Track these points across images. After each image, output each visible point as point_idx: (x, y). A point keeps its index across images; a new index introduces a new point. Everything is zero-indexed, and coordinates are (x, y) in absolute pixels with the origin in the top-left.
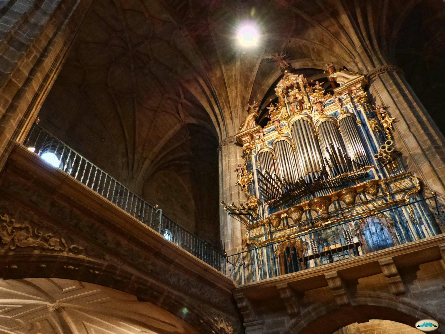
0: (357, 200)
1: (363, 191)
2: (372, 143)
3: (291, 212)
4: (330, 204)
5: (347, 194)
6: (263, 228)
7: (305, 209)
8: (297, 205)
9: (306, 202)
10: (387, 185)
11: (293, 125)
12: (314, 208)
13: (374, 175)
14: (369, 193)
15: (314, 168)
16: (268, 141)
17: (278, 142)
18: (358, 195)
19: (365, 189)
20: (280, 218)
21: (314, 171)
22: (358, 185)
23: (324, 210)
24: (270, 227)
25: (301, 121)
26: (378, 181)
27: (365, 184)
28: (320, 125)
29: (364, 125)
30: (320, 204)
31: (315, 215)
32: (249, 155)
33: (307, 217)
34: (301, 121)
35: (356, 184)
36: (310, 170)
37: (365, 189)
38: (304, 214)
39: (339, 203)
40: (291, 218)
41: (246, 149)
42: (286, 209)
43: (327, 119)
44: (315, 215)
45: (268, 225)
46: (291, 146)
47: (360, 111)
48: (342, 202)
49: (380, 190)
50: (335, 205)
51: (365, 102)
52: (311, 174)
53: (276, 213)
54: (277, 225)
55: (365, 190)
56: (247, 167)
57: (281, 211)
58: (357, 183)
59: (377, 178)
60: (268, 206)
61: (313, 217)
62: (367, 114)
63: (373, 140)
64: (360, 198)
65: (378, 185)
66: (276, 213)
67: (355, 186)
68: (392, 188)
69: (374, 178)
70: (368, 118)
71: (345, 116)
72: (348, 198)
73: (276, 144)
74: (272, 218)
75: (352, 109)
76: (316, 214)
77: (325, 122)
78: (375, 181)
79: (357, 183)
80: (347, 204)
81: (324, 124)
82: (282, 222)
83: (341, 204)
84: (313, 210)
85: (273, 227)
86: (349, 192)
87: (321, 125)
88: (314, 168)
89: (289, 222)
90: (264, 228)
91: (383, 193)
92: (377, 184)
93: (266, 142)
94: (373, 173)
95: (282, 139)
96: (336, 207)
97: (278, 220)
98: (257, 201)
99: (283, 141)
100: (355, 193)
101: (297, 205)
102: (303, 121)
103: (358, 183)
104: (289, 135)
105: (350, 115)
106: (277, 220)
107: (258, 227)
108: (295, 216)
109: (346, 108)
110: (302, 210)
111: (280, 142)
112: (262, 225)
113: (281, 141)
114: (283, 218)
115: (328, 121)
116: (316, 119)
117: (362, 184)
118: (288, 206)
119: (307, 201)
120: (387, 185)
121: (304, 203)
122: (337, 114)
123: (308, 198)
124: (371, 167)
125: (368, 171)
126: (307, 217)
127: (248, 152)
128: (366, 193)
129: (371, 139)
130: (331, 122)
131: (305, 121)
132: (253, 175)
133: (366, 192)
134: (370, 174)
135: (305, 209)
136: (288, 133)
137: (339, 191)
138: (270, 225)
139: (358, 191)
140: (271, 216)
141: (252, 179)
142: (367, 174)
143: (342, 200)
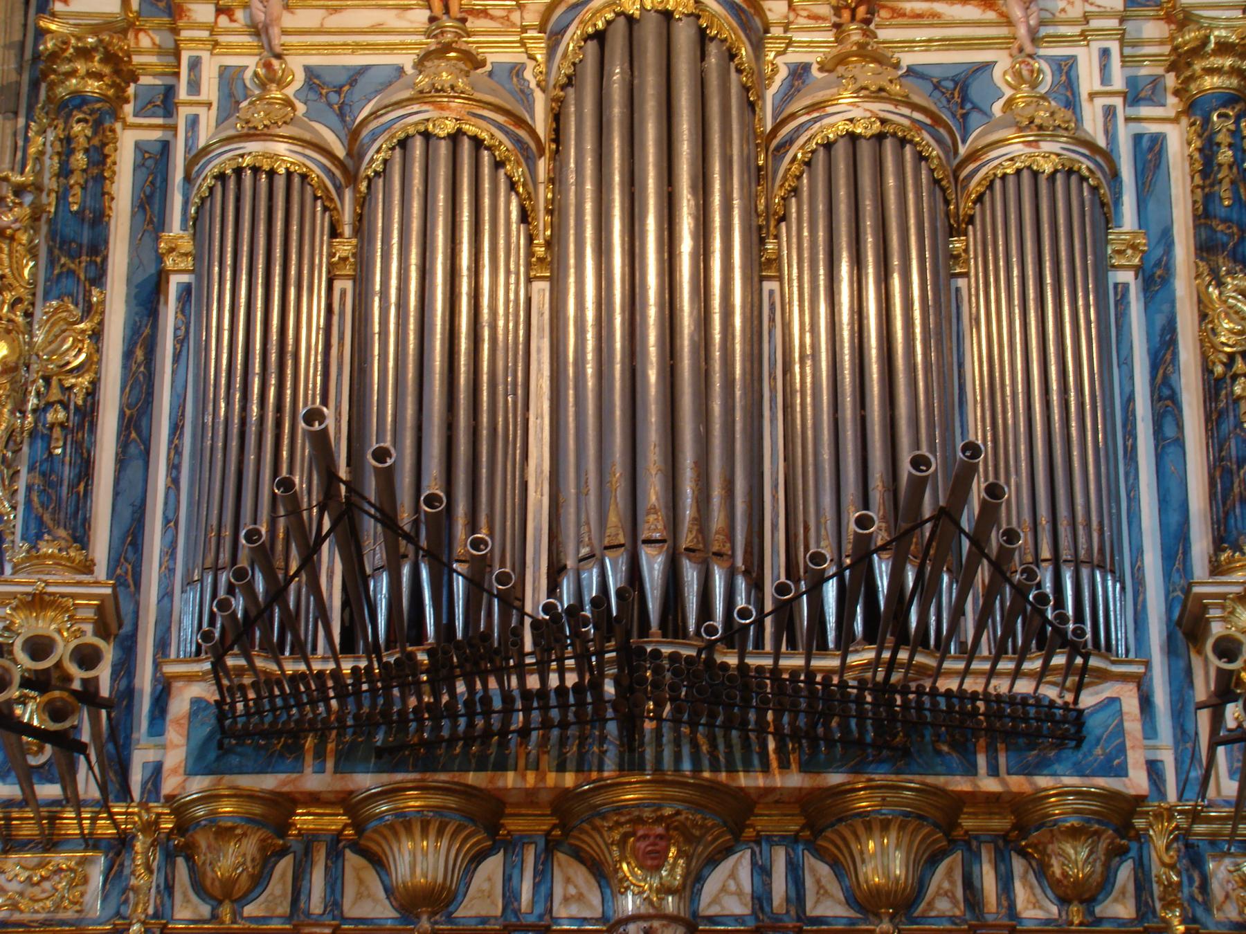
0: (940, 893)
1: (1005, 837)
2: (1170, 467)
3: (404, 824)
4: (727, 851)
5: (885, 826)
6: (97, 879)
7: (513, 825)
8: (471, 778)
9: (551, 779)
10: (1192, 857)
11: (600, 37)
12: (592, 843)
13: (1122, 750)
14: (1042, 871)
15: (688, 511)
16: (315, 60)
17: (427, 135)
18: (958, 856)
19: (1022, 828)
20: (282, 828)
21: (687, 538)
22: (990, 785)
23: (665, 890)
24: (169, 888)
25: (684, 36)
26: (1140, 799)
27: (1039, 798)
28: (828, 146)
29: (1155, 279)
30: (660, 830)
31: (580, 898)
32: (98, 125)
33: (511, 896)
34: (684, 36)
35: (971, 770)
36: (653, 526)
37: (1022, 828)
38: (493, 866)
39: (795, 872)
40: (378, 862)
41: (84, 53)
42: (366, 781)
43: (901, 117)
44: (580, 898)
45: (156, 860)
46: (524, 217)
47: (1158, 142)
48: (824, 870)
49: (1125, 873)
50: (762, 871)
51: (1230, 99)
52: (653, 566)
53: (269, 782)
54: (244, 881)
55: (1022, 831)
56: (60, 244)
57: (313, 780)
58: (981, 760)
59: (1137, 781)
60: (206, 691)
61: (560, 911)
62: (1203, 216)
63: (1180, 442)
64: (970, 885)
65: (1125, 828)
66: (269, 782)
67: (961, 784)
68: (1216, 887)
69: (1121, 771)
70: (1205, 249)
71: (1049, 154)
72: (884, 860)
73: (403, 144)
74: (213, 817)
75: (1109, 112)
76: (595, 899)
77: (880, 137)
78: (1111, 797)
79: (981, 760)
80: (852, 900)
81: (865, 149)
82: (285, 865)
83: (809, 883)
84: (579, 856)
85: (199, 886)
86: (909, 820)
87: (841, 151)
88: (688, 511)
89: (350, 891)
90: (113, 875)
91: (1144, 907)
92: (1119, 820)
93: (296, 65)
94: (1120, 731)
95: (470, 129)
96: (761, 899)
97: (263, 848)
98: (100, 610)
99: (477, 143)
100: (942, 829)
101: (471, 778)
102: (703, 38)
103: (994, 771)
104: (526, 97)
105: (1085, 165)
106: (250, 846)
107: (51, 842)
108: (419, 860)
109: (1066, 70)
110: (493, 828)
111: (443, 149)
112: (91, 842)
113: (455, 138)
114: (309, 840)
115: (903, 142)
116: (794, 57)
117: (1018, 783)
118: (388, 758)
119: (561, 768)
120: (1193, 856)
121: (531, 779)
122: (975, 92)
123: (572, 750)
124: (1124, 678)
125: (1088, 700)
126: (511, 896)
127: (93, 86)
128: (1018, 864)
129: (1170, 431)
130: (920, 157)
131: (713, 48)
132: (97, 335)
133: (1023, 853)
134: (1094, 725)
135: (513, 825)
136: (516, 70)
137: (835, 779)
138: (170, 857)
139: (967, 823)
140: (209, 798)
141: (85, 381)
142: (1078, 718)
143: (820, 854)
